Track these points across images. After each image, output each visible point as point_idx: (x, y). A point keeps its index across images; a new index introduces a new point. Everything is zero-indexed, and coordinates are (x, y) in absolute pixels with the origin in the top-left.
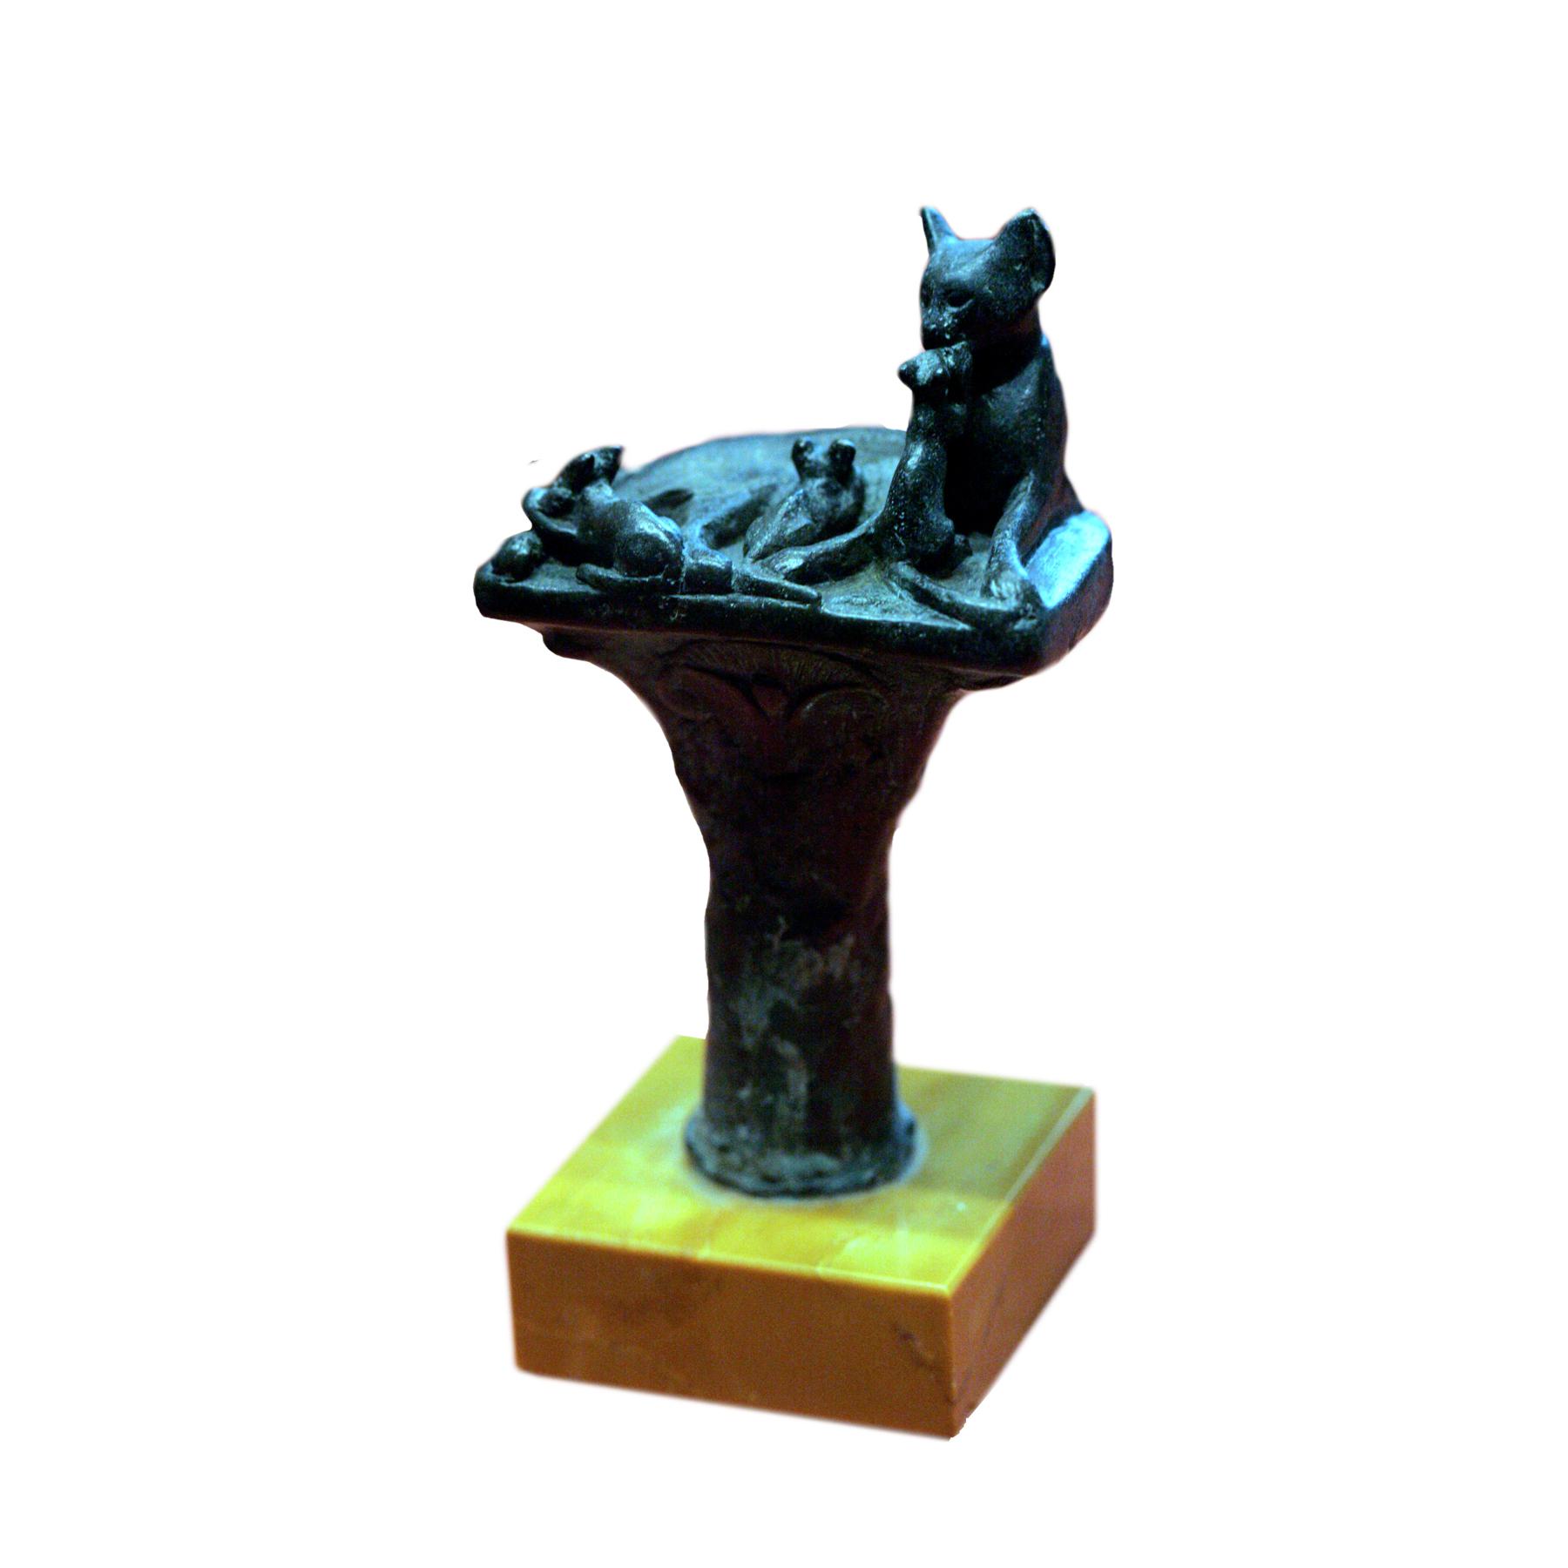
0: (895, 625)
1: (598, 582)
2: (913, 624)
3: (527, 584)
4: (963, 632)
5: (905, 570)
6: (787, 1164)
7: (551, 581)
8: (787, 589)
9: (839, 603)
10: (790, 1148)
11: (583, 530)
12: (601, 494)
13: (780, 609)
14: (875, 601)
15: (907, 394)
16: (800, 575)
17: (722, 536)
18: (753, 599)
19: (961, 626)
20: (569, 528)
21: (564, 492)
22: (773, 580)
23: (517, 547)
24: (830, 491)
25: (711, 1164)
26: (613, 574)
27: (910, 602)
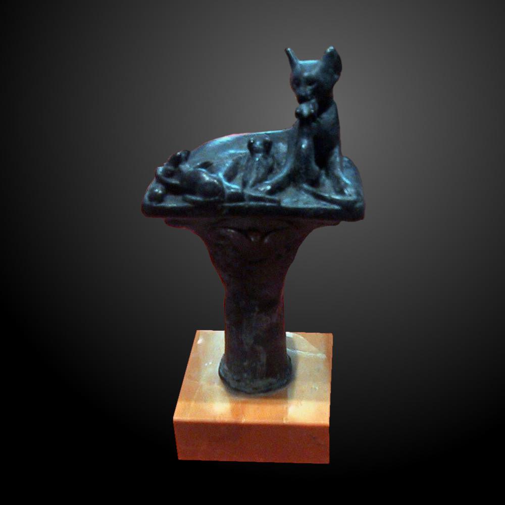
0: (311, 209)
1: (194, 202)
2: (317, 208)
3: (163, 204)
4: (337, 210)
5: (305, 186)
6: (260, 383)
7: (172, 203)
8: (267, 199)
9: (287, 200)
10: (262, 378)
11: (181, 181)
12: (186, 167)
13: (265, 207)
14: (297, 199)
15: (295, 120)
16: (271, 192)
17: (230, 177)
18: (252, 203)
19: (336, 207)
20: (174, 181)
21: (171, 168)
22: (260, 195)
23: (157, 190)
24: (265, 158)
25: (233, 384)
26: (198, 198)
27: (311, 199)
